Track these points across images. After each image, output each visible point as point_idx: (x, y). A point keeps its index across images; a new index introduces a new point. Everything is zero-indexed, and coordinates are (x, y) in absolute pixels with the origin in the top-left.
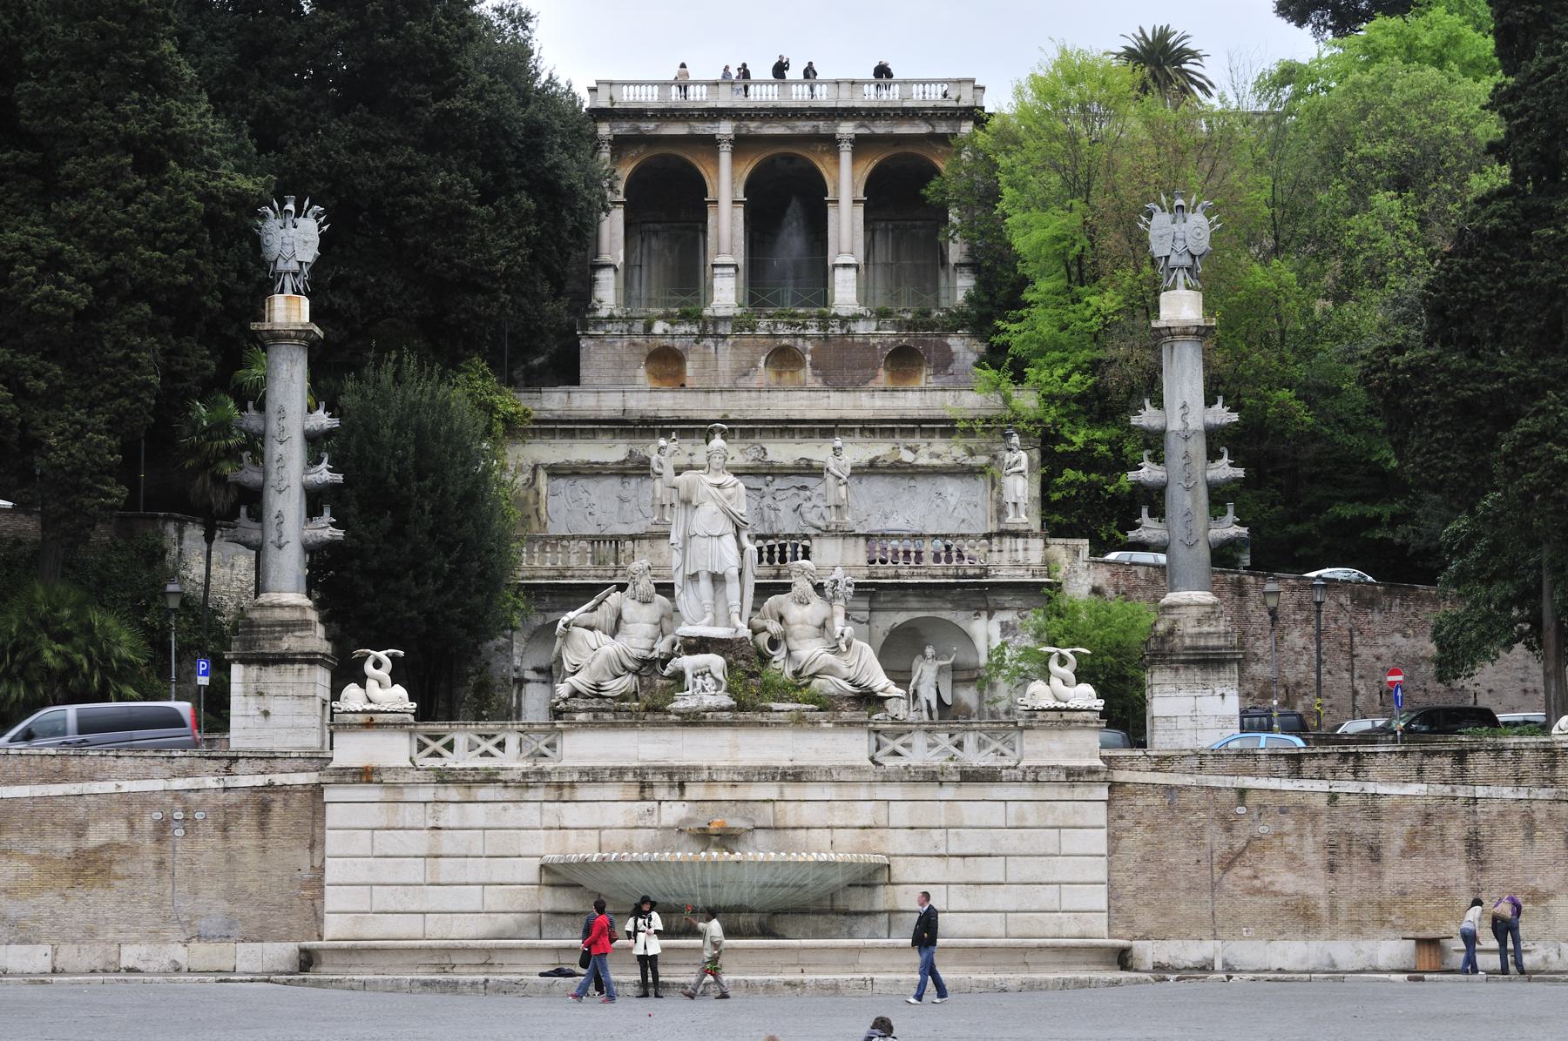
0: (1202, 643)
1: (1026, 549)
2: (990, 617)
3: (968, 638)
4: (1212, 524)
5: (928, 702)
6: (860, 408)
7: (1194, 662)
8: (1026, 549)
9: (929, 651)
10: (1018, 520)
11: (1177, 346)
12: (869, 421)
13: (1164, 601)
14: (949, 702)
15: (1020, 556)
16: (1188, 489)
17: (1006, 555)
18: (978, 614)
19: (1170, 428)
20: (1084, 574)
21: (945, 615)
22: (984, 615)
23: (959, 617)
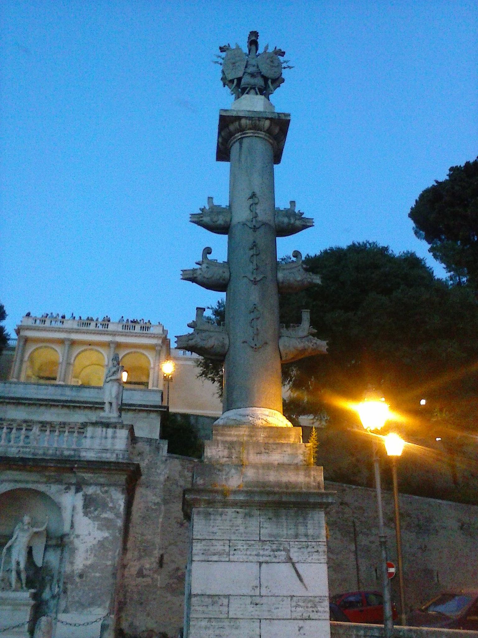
0: (272, 477)
1: (114, 437)
2: (77, 491)
3: (58, 507)
4: (284, 331)
5: (18, 563)
6: (65, 395)
7: (262, 506)
8: (114, 437)
9: (26, 519)
10: (111, 415)
11: (246, 142)
12: (67, 401)
13: (222, 296)
14: (39, 563)
15: (108, 444)
16: (255, 282)
17: (97, 441)
18: (68, 489)
19: (235, 220)
20: (162, 466)
21: (42, 488)
22: (73, 488)
23: (53, 490)
